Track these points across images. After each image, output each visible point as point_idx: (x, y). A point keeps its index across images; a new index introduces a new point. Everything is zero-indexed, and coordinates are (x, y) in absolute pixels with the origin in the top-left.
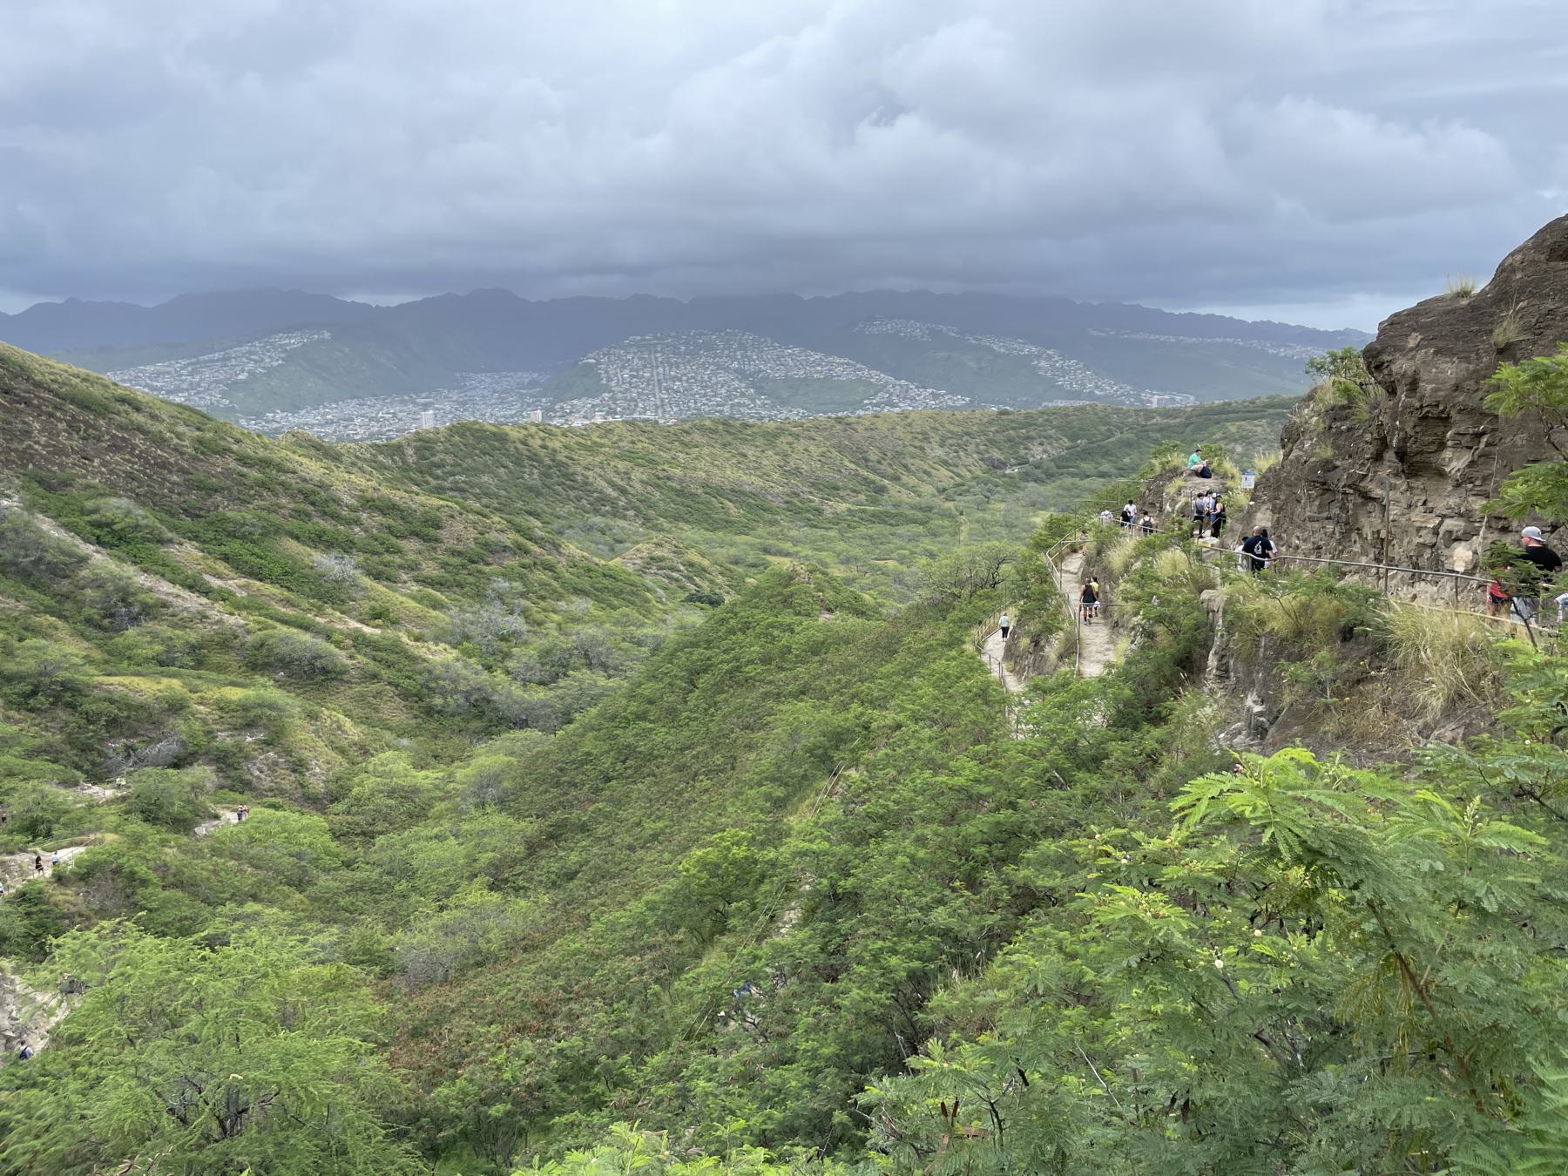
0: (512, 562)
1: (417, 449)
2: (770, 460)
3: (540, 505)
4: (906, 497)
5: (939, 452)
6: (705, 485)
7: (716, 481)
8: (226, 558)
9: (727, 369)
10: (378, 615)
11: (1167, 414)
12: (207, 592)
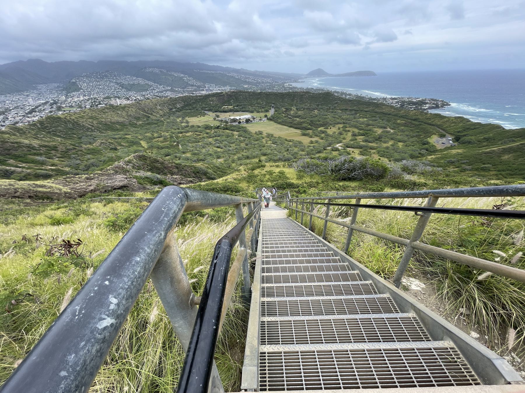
0: (74, 151)
1: (40, 124)
2: (124, 114)
3: (75, 132)
4: (154, 118)
5: (159, 108)
6: (111, 122)
7: (113, 121)
8: (20, 161)
9: (112, 82)
10: (53, 165)
11: (200, 96)
12: (20, 167)
